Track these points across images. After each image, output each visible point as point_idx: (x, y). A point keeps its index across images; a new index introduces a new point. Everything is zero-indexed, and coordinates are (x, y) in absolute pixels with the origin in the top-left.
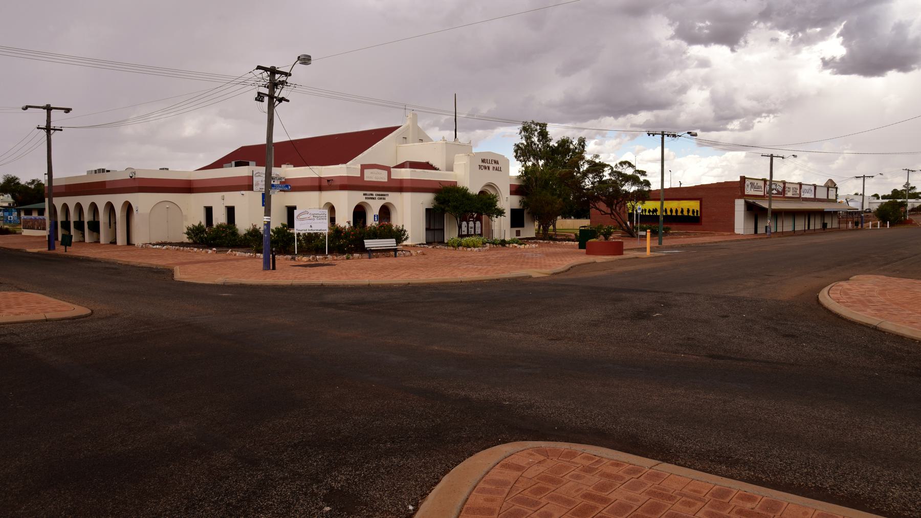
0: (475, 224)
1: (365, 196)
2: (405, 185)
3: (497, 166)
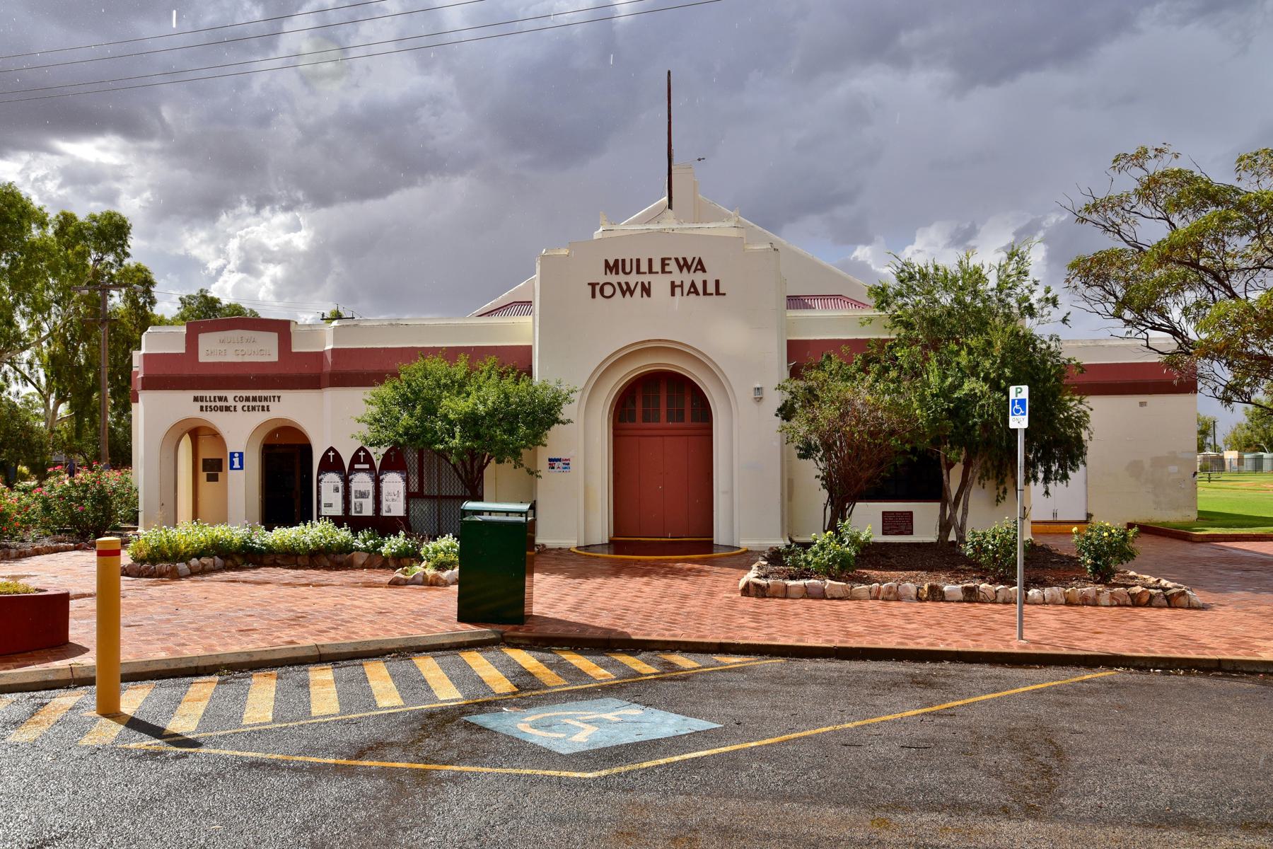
0: (377, 483)
1: (200, 404)
3: (698, 278)
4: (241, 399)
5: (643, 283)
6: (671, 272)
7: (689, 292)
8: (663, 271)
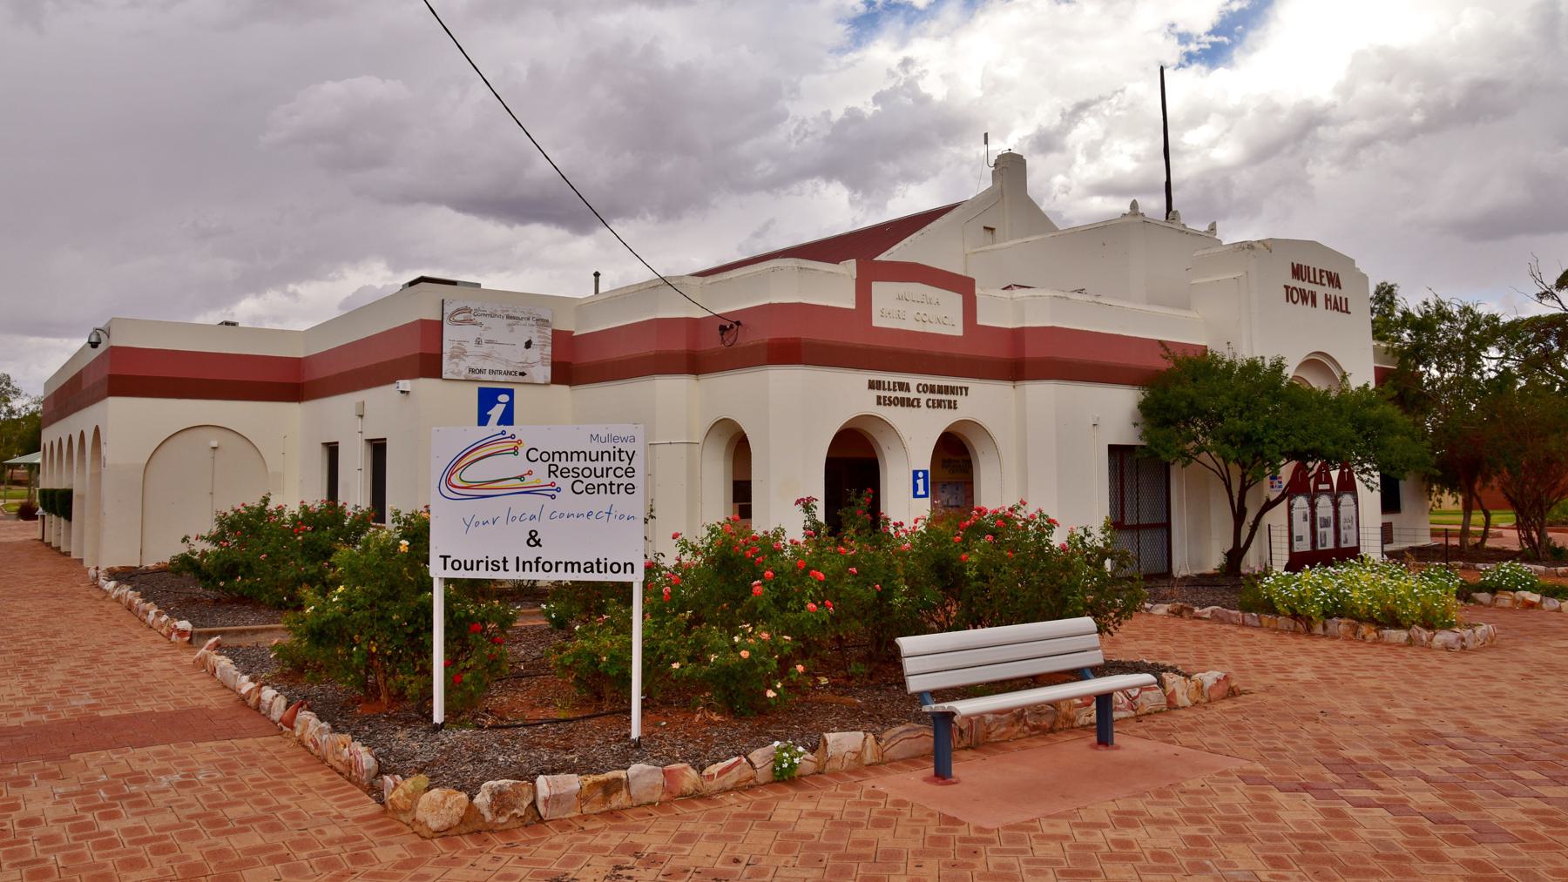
0: (1336, 505)
1: (876, 393)
2: (1032, 351)
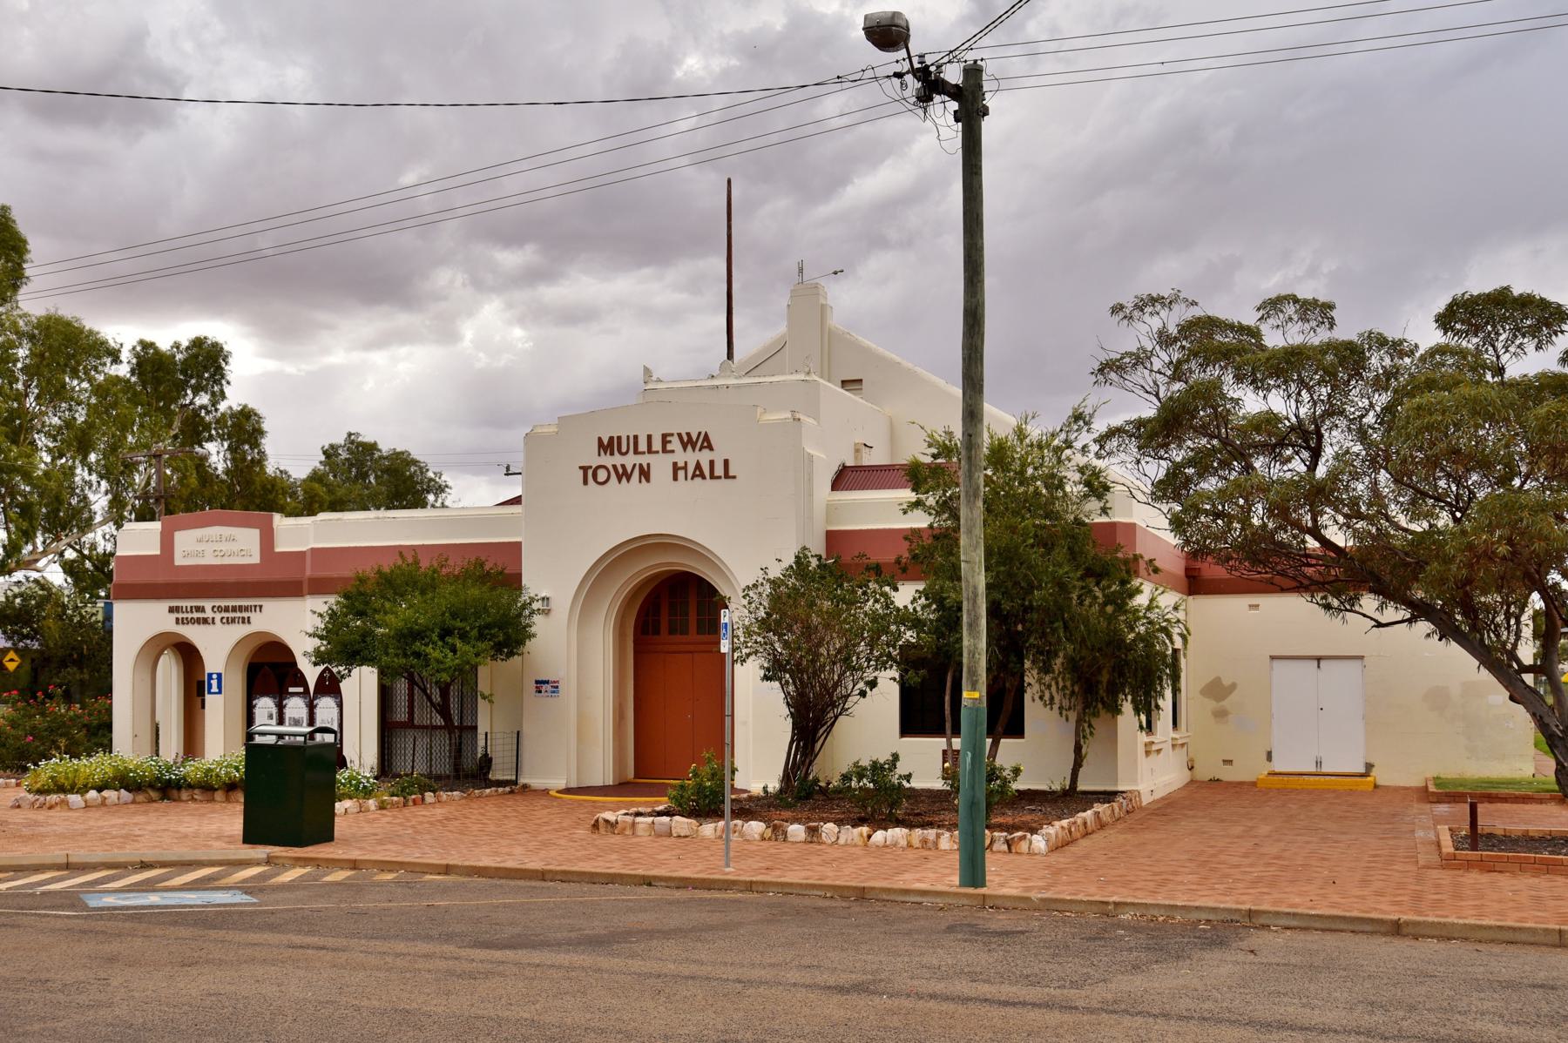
0: (311, 708)
1: (176, 615)
3: (704, 457)
4: (220, 609)
5: (641, 465)
6: (673, 451)
7: (694, 476)
8: (665, 450)
